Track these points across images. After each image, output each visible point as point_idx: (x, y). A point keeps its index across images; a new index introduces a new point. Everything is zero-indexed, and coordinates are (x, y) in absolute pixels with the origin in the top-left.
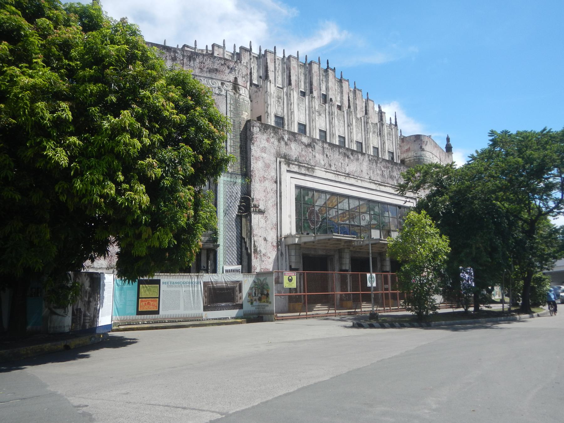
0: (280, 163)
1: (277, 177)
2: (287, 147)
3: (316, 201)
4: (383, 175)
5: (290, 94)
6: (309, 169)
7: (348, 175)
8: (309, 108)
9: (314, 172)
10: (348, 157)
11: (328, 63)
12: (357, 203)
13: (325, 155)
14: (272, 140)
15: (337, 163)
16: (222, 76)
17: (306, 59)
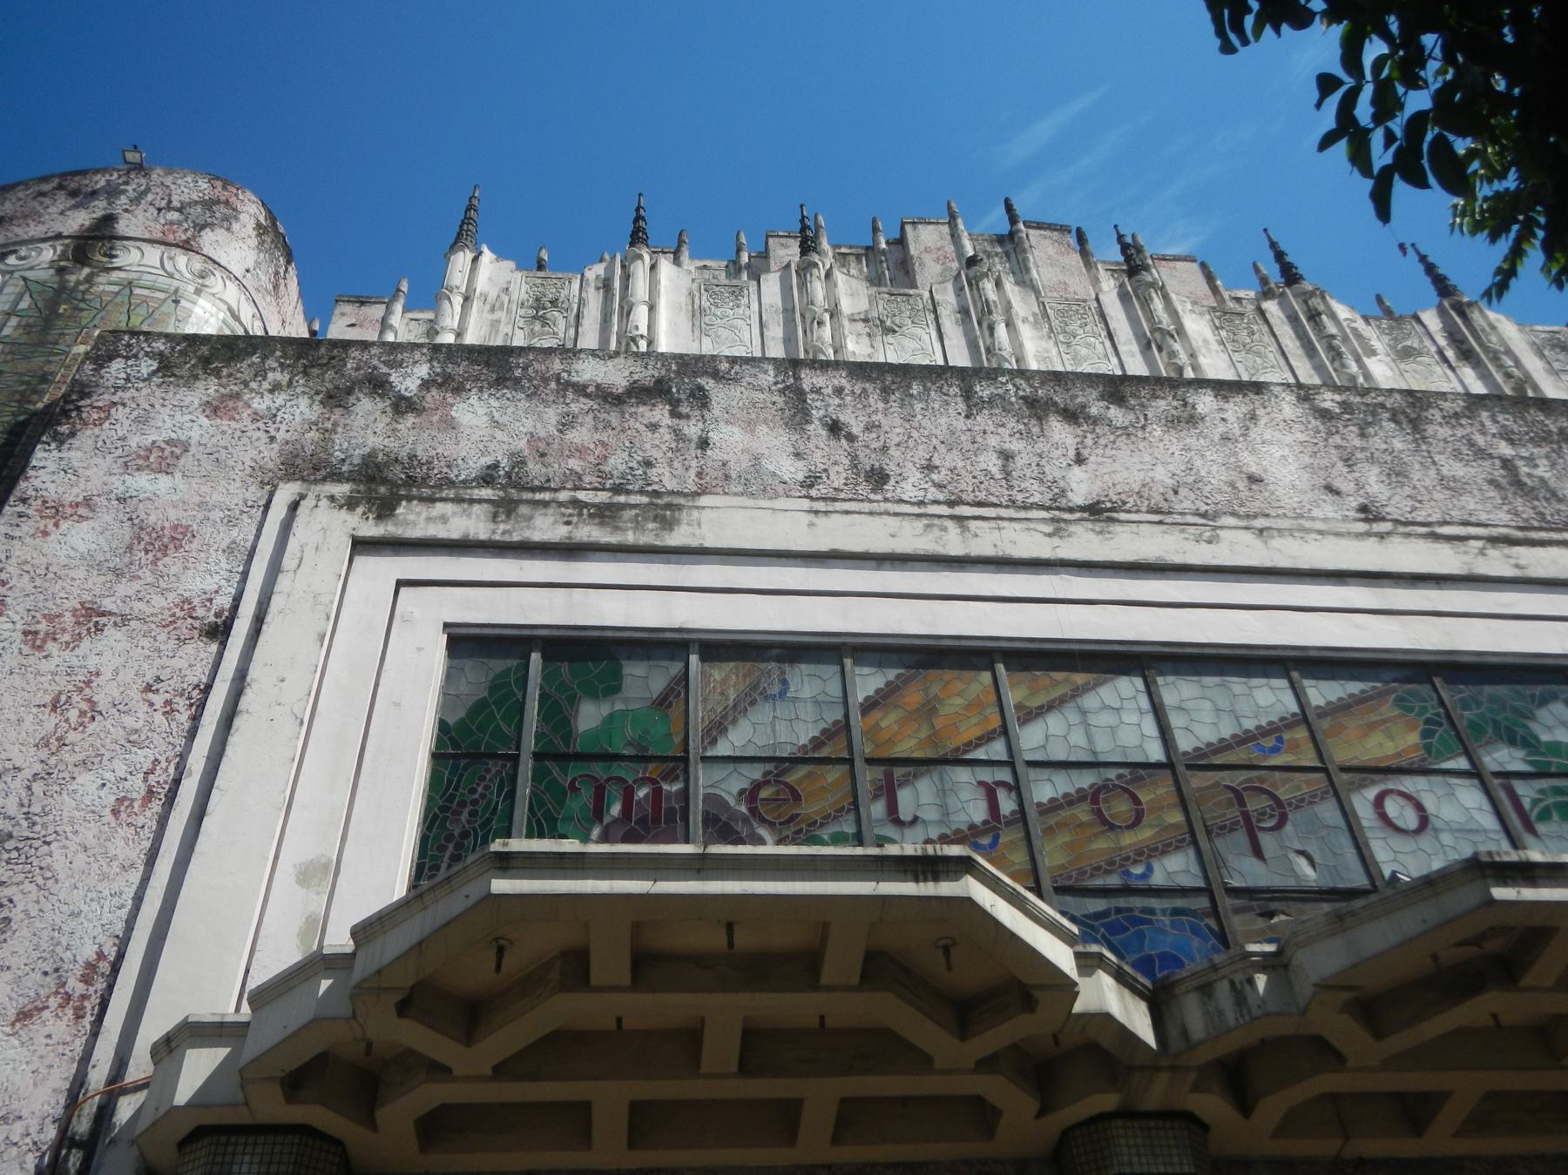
0: (294, 507)
1: (237, 599)
2: (411, 419)
3: (717, 729)
4: (1513, 482)
5: (626, 277)
6: (632, 521)
7: (1098, 512)
8: (788, 311)
9: (668, 524)
10: (1072, 416)
11: (1009, 208)
12: (1269, 699)
13: (816, 428)
14: (260, 404)
15: (948, 460)
16: (16, 230)
17: (875, 230)
